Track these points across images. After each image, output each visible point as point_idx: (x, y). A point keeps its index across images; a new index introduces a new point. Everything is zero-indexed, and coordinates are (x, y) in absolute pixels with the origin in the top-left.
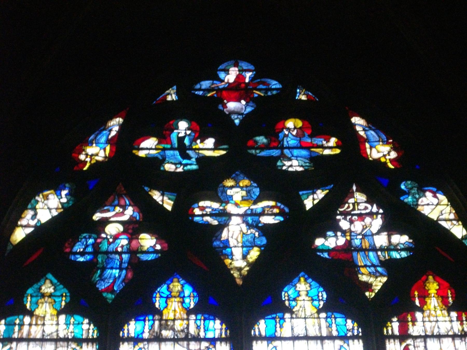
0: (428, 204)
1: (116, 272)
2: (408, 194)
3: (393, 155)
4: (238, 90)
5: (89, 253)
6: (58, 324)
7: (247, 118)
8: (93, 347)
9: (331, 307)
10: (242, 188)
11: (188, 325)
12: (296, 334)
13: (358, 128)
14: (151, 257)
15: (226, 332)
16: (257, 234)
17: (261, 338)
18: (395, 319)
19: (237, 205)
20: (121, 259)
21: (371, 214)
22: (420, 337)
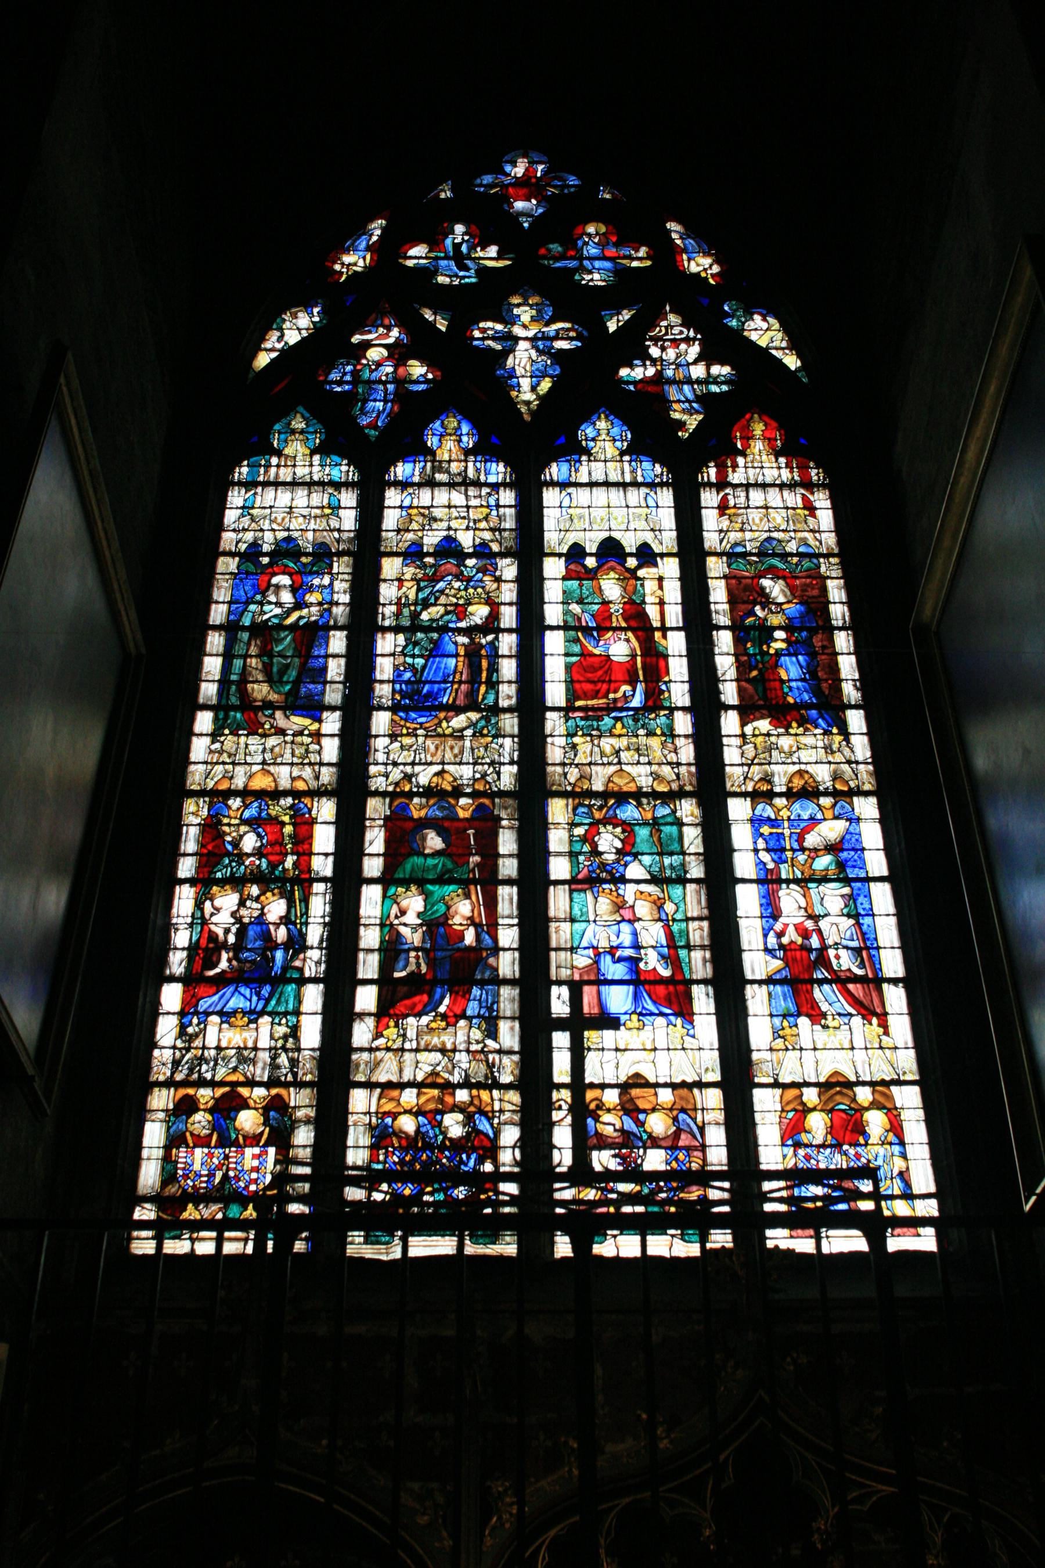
0: (756, 329)
1: (380, 405)
2: (733, 317)
3: (716, 269)
4: (527, 186)
5: (347, 383)
6: (311, 465)
7: (537, 221)
9: (634, 450)
10: (531, 306)
11: (466, 468)
12: (594, 480)
13: (674, 236)
14: (422, 387)
15: (511, 476)
16: (549, 362)
17: (553, 484)
18: (712, 464)
19: (525, 326)
20: (386, 389)
21: (687, 340)
22: (741, 485)
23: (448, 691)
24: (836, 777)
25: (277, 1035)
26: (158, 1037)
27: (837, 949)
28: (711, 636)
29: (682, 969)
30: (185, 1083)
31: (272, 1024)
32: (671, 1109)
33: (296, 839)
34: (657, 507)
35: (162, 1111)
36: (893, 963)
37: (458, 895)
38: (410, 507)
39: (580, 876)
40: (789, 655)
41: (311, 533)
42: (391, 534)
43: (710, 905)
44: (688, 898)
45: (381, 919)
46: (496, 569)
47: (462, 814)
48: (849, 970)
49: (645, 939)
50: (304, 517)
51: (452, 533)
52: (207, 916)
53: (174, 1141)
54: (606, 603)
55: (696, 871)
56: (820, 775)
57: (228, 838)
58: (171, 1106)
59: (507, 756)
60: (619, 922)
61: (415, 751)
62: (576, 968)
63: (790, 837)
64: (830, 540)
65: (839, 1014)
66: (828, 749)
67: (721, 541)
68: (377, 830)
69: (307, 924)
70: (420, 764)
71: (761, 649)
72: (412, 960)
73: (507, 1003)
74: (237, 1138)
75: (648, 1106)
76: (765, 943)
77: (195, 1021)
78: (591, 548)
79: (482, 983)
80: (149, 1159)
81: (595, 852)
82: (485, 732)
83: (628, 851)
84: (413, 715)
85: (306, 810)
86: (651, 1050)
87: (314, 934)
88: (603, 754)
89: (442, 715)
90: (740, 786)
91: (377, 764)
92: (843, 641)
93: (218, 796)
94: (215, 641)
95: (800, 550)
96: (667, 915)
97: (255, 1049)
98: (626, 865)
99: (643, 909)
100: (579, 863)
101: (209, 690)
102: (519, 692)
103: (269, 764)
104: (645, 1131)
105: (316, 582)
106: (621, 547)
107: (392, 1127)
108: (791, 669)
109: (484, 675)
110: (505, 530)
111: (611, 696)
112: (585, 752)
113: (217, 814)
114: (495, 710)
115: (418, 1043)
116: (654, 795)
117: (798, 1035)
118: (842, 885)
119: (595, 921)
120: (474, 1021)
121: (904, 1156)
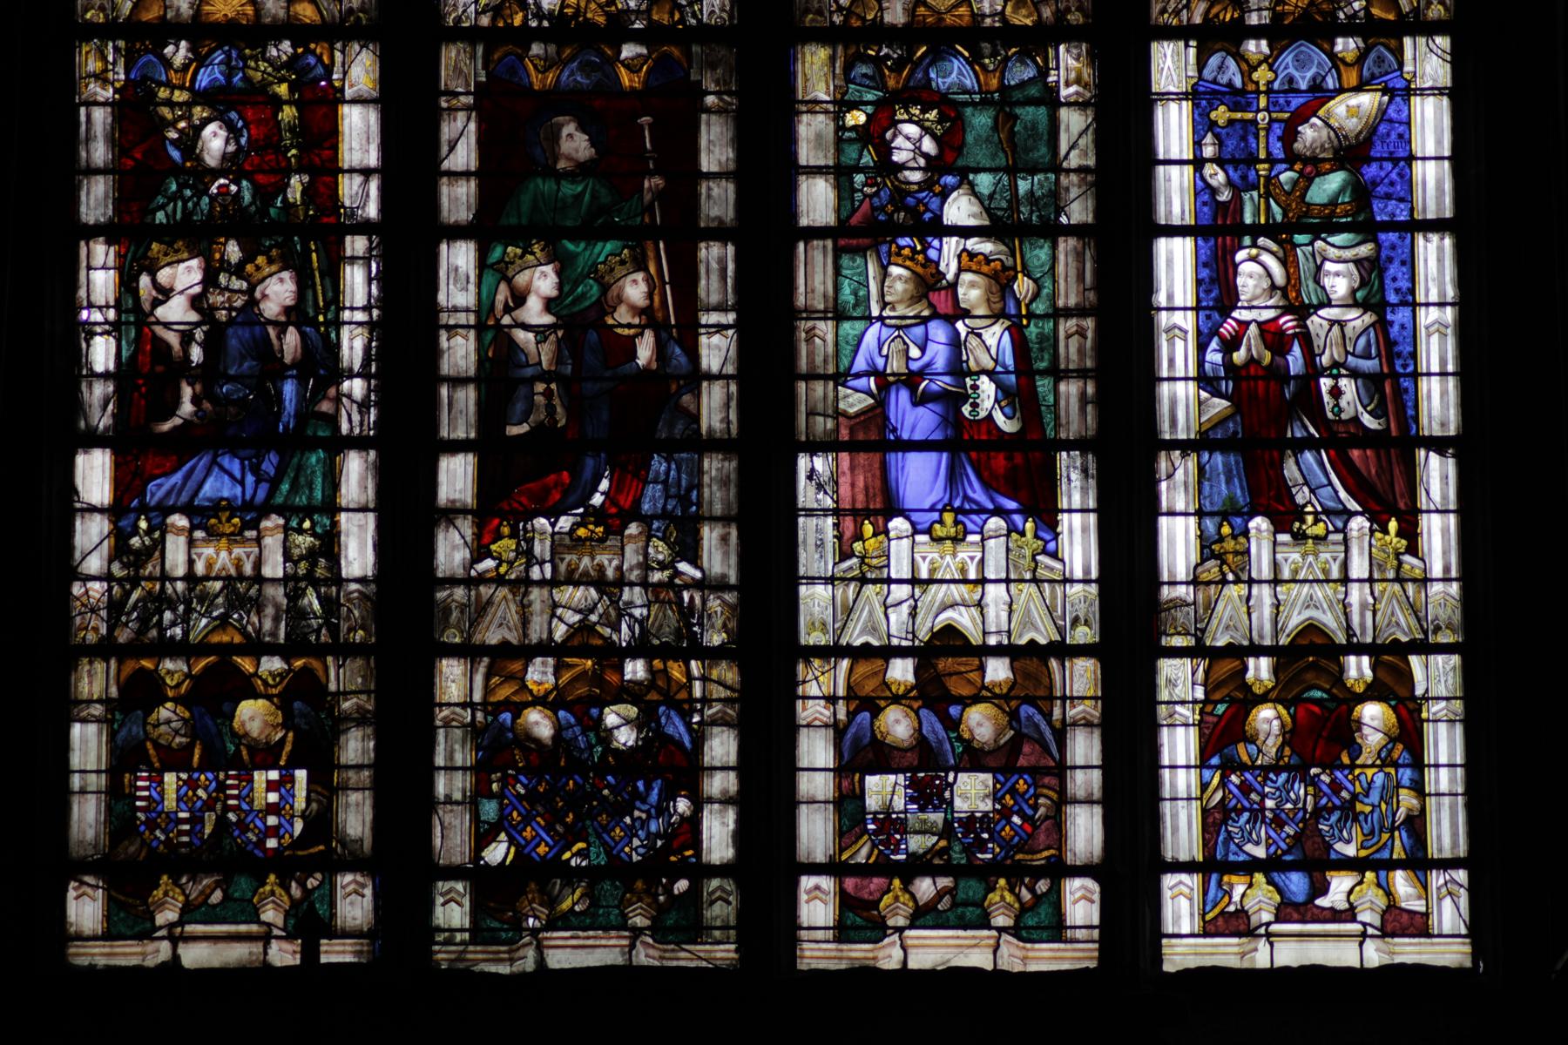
25: (296, 552)
26: (78, 555)
27: (1336, 377)
29: (1041, 417)
30: (136, 649)
31: (286, 529)
32: (1006, 697)
33: (301, 130)
35: (99, 701)
36: (1438, 404)
37: (623, 263)
39: (854, 221)
43: (1098, 286)
44: (1061, 268)
45: (478, 313)
47: (626, 78)
48: (1356, 420)
49: (978, 357)
52: (146, 306)
53: (125, 759)
55: (1078, 211)
57: (173, 135)
58: (114, 692)
60: (924, 321)
62: (845, 414)
63: (1268, 130)
65: (1328, 512)
68: (461, 116)
69: (338, 324)
72: (539, 399)
73: (715, 488)
74: (238, 751)
75: (965, 691)
76: (1201, 362)
77: (143, 525)
79: (669, 449)
80: (83, 792)
81: (887, 167)
83: (948, 165)
85: (320, 70)
86: (975, 582)
87: (353, 346)
90: (1177, 13)
96: (1018, 302)
97: (258, 579)
98: (944, 195)
99: (972, 292)
100: (855, 191)
104: (960, 738)
107: (512, 729)
113: (145, 78)
115: (555, 569)
116: (1007, 34)
117: (1248, 551)
118: (1359, 238)
119: (881, 318)
120: (656, 525)
121: (1418, 788)
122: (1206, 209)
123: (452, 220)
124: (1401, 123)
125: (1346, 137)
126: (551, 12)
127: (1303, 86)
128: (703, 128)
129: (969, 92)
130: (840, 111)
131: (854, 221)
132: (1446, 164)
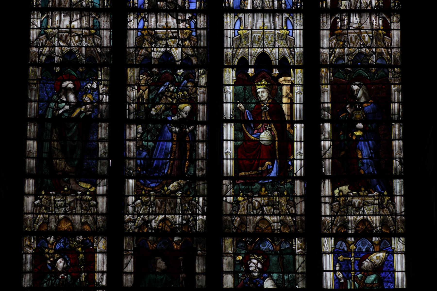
8: (108, 17)
22: (345, 11)
23: (168, 165)
24: (383, 223)
28: (320, 126)
34: (293, 29)
38: (143, 29)
39: (239, 287)
40: (364, 141)
41: (84, 48)
42: (132, 50)
46: (195, 77)
50: (79, 35)
51: (168, 49)
54: (259, 102)
56: (374, 222)
57: (49, 262)
59: (200, 209)
61: (149, 206)
63: (354, 262)
64: (396, 52)
66: (381, 206)
67: (330, 55)
70: (152, 214)
71: (348, 136)
78: (251, 61)
81: (248, 272)
82: (189, 193)
83: (265, 272)
84: (149, 182)
85: (90, 244)
88: (254, 208)
89: (164, 182)
90: (329, 230)
91: (128, 214)
92: (396, 130)
93: (41, 235)
94: (32, 129)
95: (378, 62)
101: (31, 163)
102: (207, 165)
103: (68, 214)
105: (89, 86)
106: (270, 61)
108: (364, 151)
109: (188, 154)
110: (201, 47)
111: (260, 169)
112: (244, 207)
114: (194, 179)
116: (281, 235)
122: (337, 284)
123: (126, 286)
124: (391, 261)
125: (376, 265)
126: (155, 228)
127: (364, 251)
128: (197, 260)
129: (271, 251)
130: (235, 256)
131: (239, 287)
132: (404, 273)
